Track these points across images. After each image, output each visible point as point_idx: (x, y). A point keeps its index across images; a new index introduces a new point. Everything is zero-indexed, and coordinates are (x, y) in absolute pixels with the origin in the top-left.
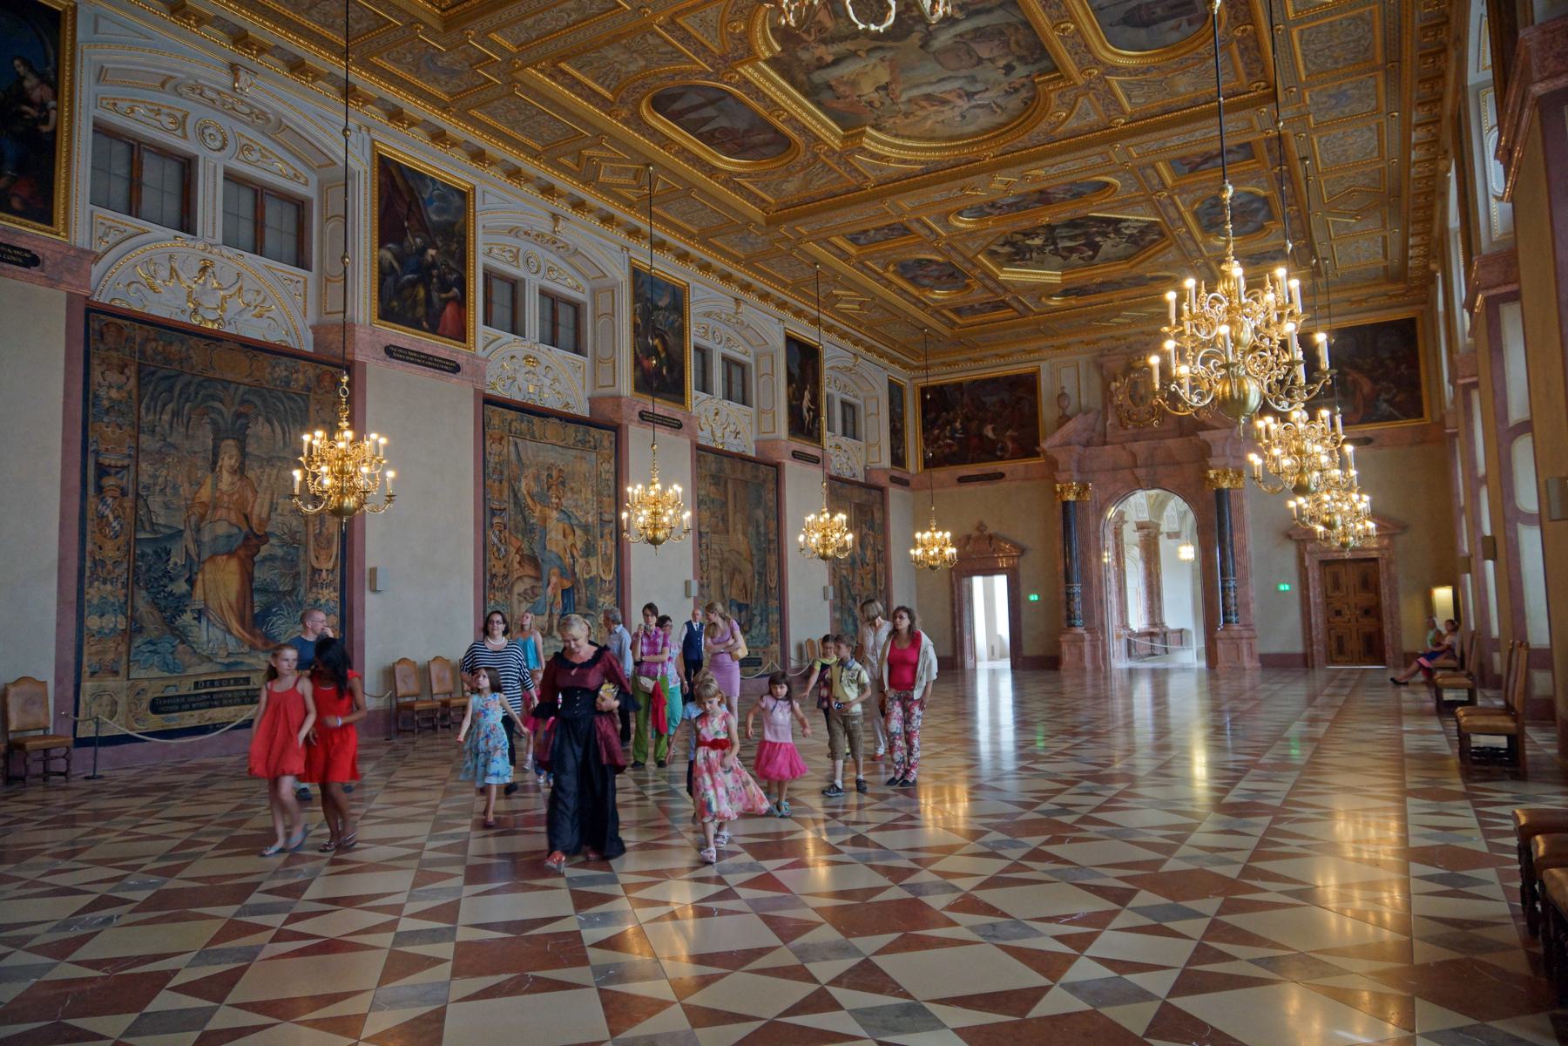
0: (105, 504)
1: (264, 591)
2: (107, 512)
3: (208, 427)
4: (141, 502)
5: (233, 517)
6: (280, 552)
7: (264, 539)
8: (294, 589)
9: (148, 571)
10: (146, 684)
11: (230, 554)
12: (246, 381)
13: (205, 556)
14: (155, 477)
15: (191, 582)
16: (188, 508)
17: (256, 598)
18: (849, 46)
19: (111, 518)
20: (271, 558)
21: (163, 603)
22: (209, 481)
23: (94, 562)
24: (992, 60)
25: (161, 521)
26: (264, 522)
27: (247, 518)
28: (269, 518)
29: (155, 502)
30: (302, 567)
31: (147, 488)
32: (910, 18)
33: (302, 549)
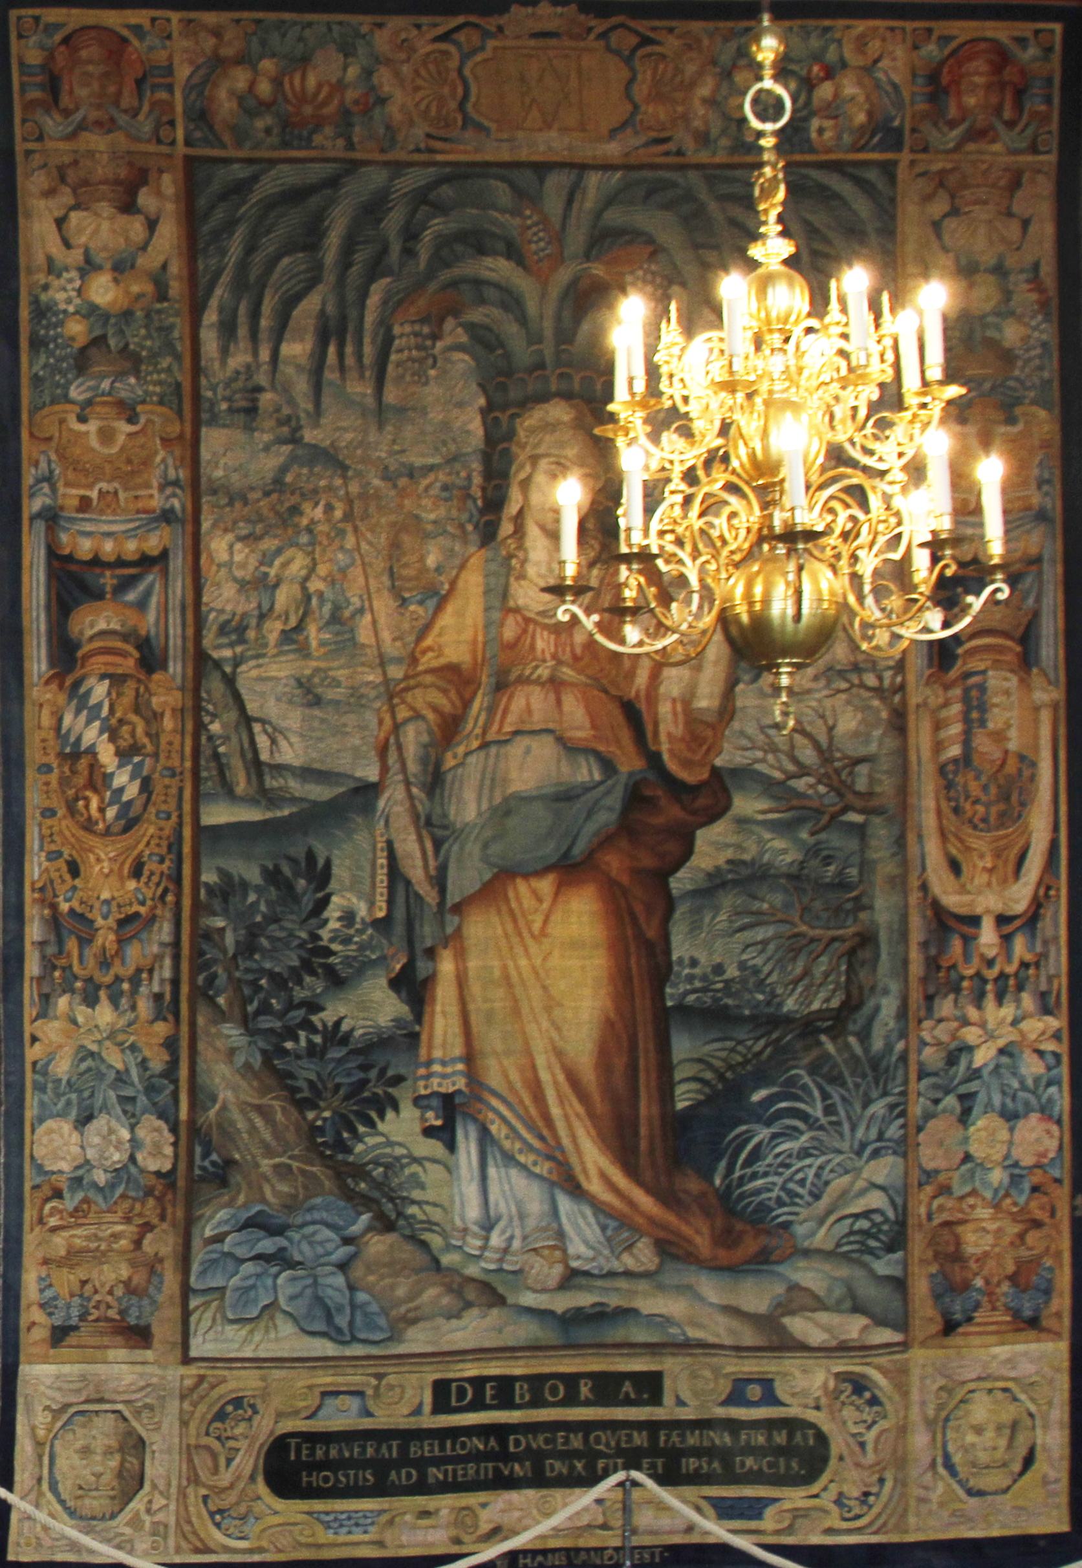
0: (81, 701)
1: (713, 1016)
2: (91, 735)
3: (462, 361)
4: (215, 686)
5: (575, 715)
6: (782, 852)
7: (712, 796)
8: (851, 1006)
9: (248, 947)
10: (246, 1382)
11: (569, 870)
12: (612, 149)
13: (466, 878)
14: (263, 584)
15: (414, 988)
16: (392, 693)
17: (682, 1046)
19: (107, 755)
20: (744, 877)
21: (307, 1071)
22: (473, 582)
23: (55, 922)
25: (290, 753)
26: (704, 731)
27: (633, 715)
28: (727, 710)
29: (267, 682)
30: (883, 910)
31: (234, 630)
33: (881, 833)
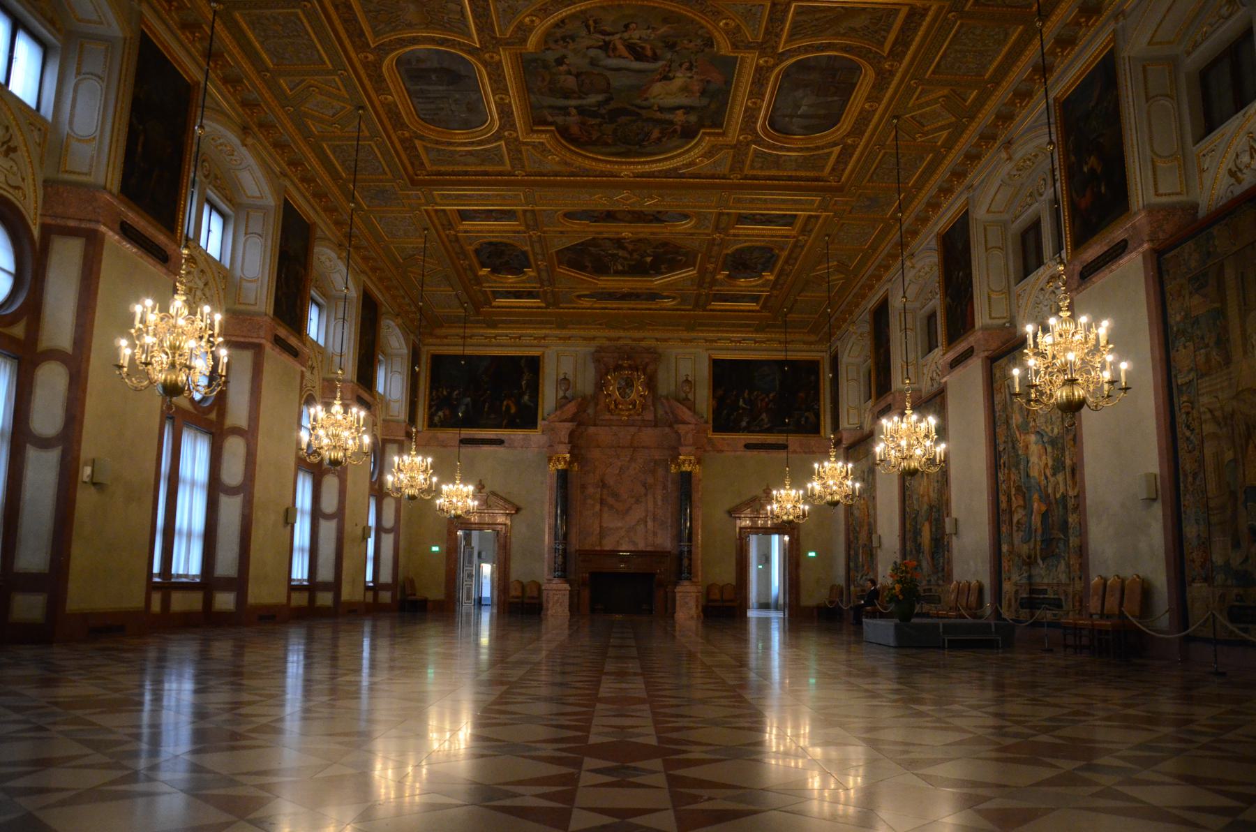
18: (659, 115)
24: (569, 73)
32: (603, 118)
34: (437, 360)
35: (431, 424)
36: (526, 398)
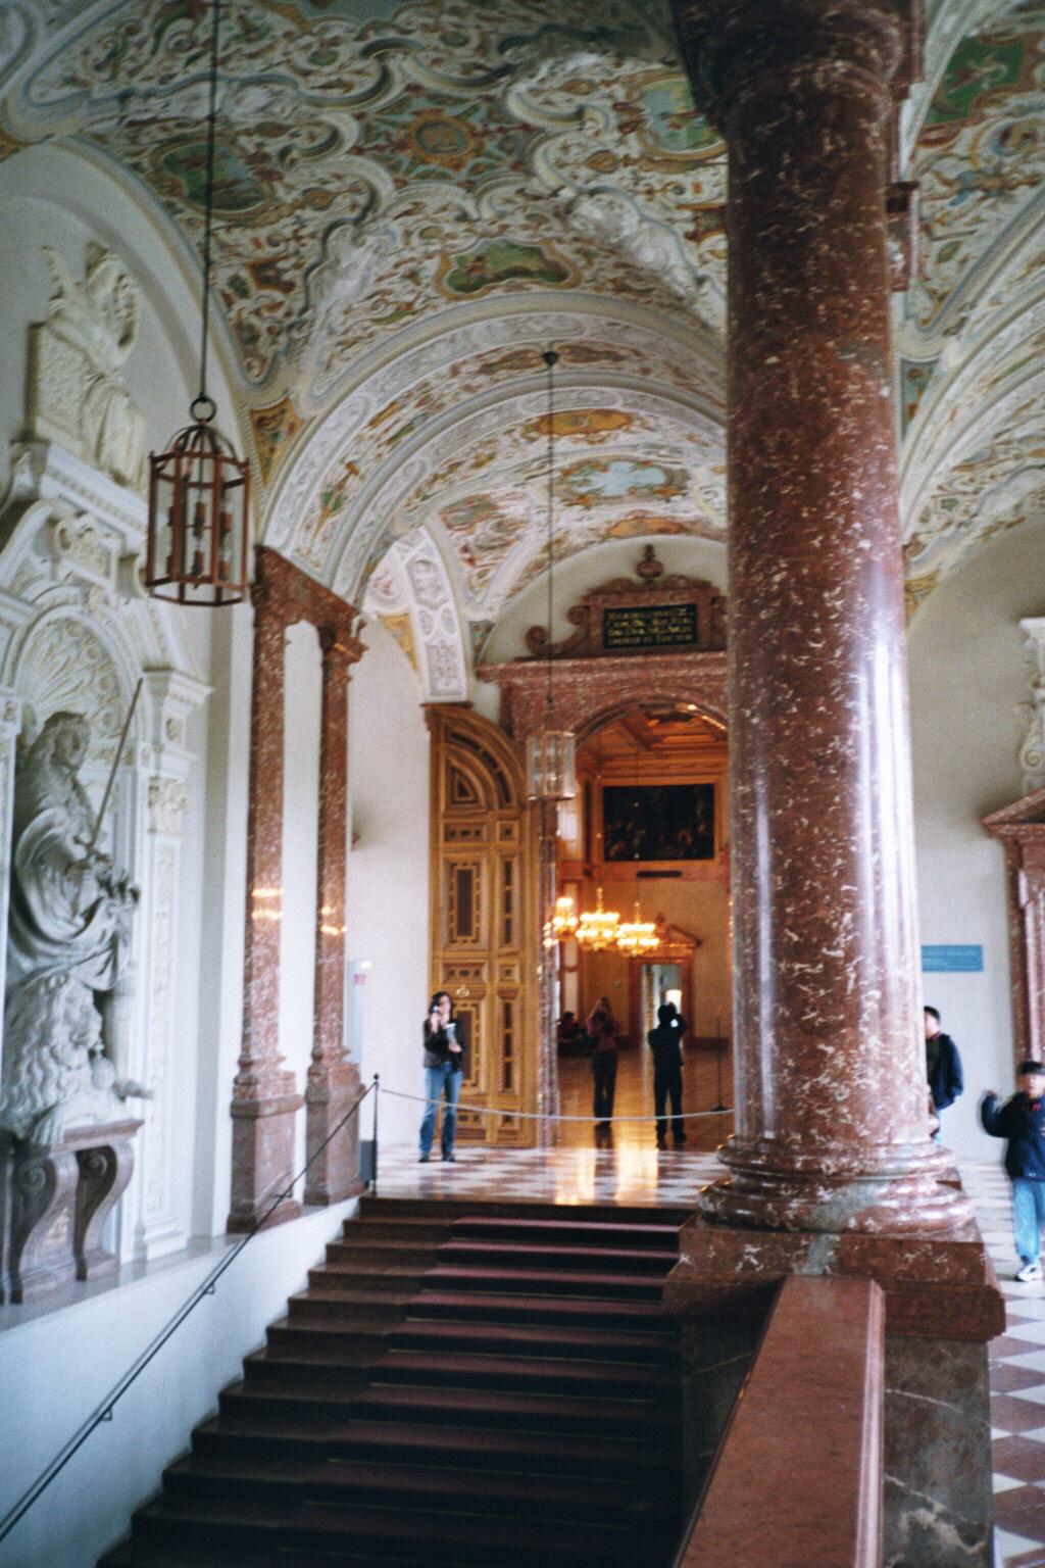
34: (612, 795)
35: (607, 859)
36: (701, 828)
